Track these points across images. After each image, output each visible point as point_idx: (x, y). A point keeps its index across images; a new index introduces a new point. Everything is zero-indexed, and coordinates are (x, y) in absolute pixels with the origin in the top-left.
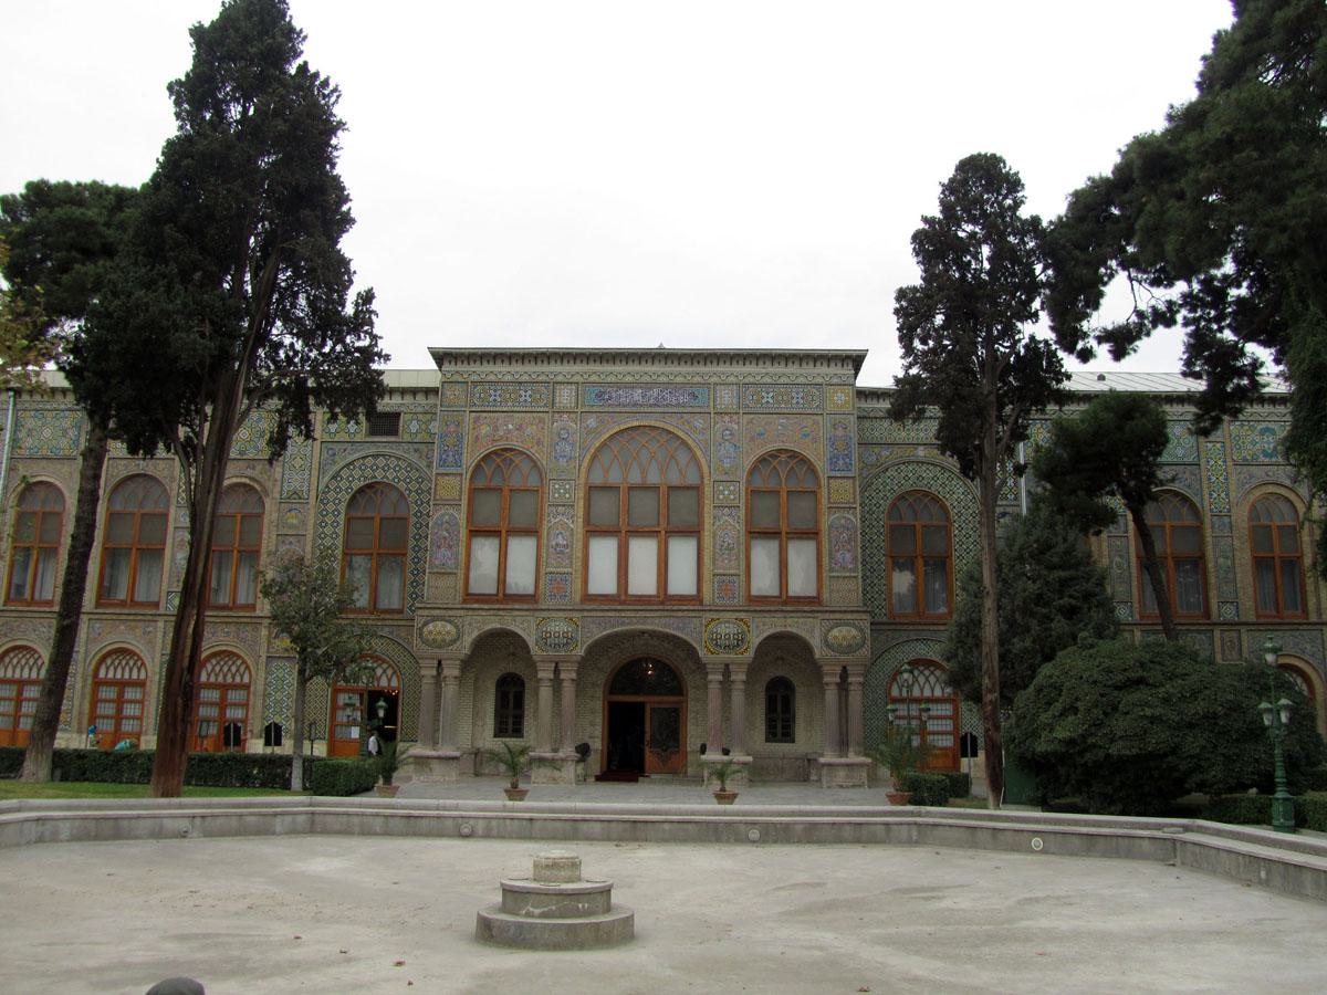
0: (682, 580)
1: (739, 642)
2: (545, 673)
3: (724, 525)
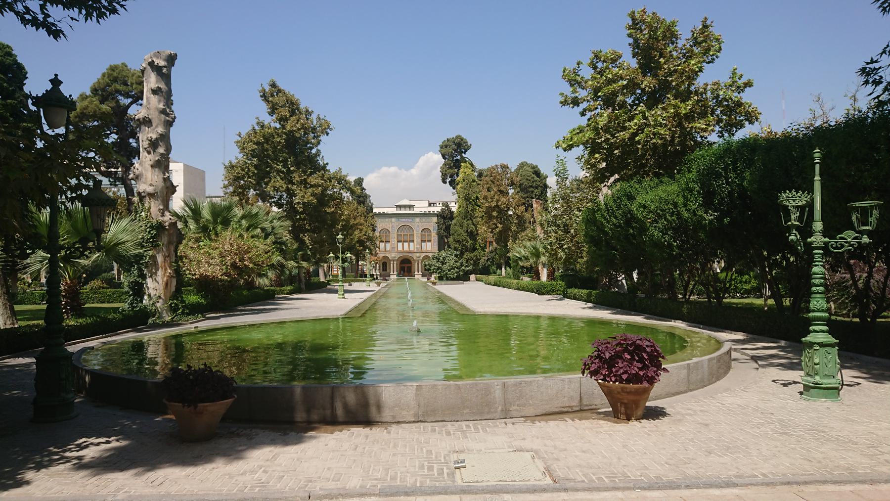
0: (412, 248)
1: (420, 257)
2: (392, 262)
3: (417, 239)
